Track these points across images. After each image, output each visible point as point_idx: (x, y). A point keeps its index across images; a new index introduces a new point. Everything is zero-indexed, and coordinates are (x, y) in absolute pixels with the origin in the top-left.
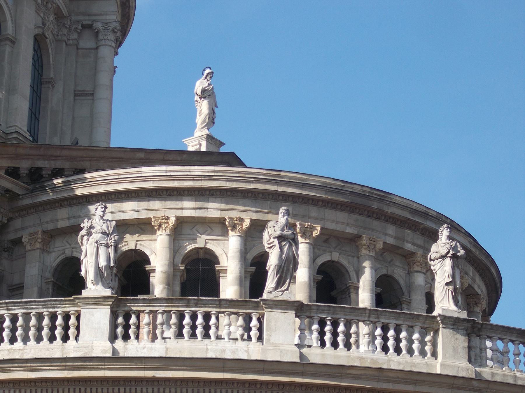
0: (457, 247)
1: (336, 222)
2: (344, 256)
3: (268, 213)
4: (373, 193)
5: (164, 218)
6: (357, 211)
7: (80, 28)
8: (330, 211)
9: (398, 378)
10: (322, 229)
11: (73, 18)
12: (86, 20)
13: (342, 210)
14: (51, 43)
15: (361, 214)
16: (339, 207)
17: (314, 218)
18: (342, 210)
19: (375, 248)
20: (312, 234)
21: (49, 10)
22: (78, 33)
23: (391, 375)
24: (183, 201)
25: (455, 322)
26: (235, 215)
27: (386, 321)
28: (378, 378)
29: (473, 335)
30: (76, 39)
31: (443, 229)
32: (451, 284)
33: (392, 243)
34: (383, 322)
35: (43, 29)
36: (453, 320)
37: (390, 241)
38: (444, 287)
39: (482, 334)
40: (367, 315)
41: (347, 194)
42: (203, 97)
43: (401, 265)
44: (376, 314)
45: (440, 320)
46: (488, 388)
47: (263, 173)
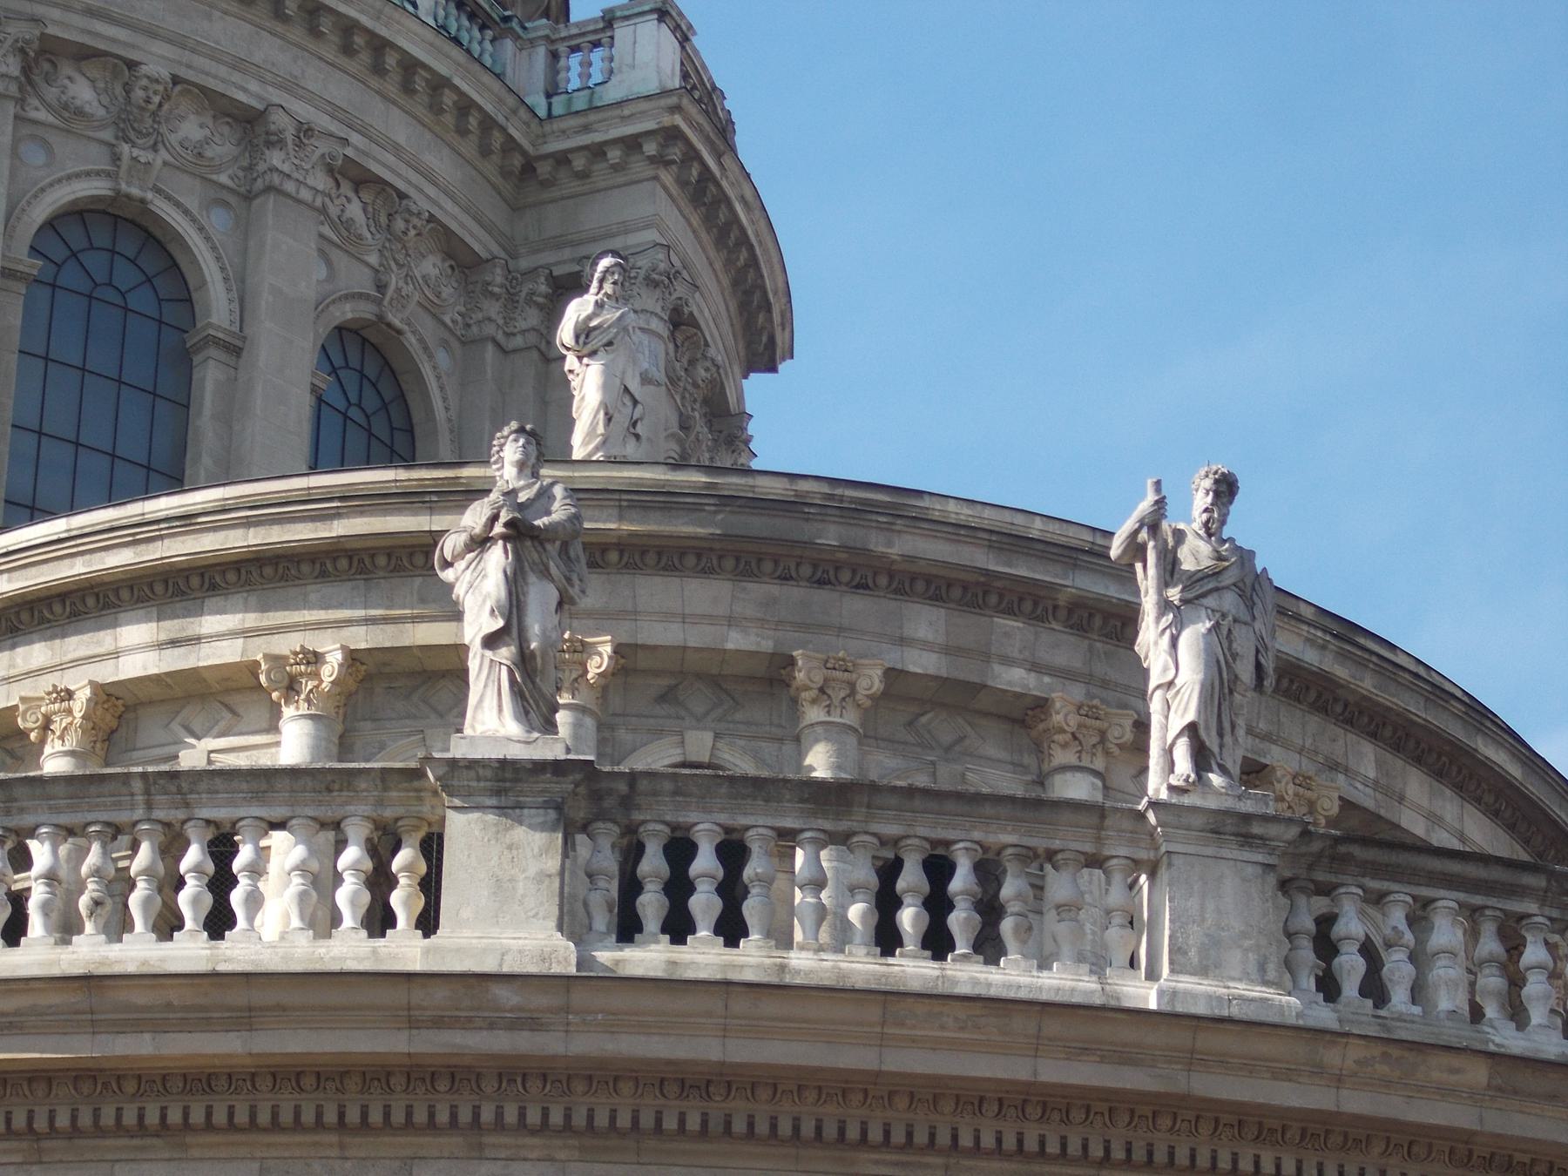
0: (552, 498)
1: (684, 619)
2: (742, 743)
3: (415, 619)
4: (841, 499)
5: (54, 695)
6: (768, 566)
7: (543, 288)
8: (657, 580)
9: (169, 1006)
10: (618, 650)
11: (524, 263)
12: (564, 262)
13: (707, 572)
14: (426, 349)
15: (786, 579)
16: (691, 560)
17: (590, 614)
18: (703, 571)
19: (853, 692)
20: (586, 672)
21: (399, 240)
22: (541, 307)
23: (140, 998)
24: (120, 626)
25: (504, 780)
26: (286, 645)
27: (222, 814)
28: (89, 1017)
29: (600, 824)
30: (533, 329)
31: (502, 440)
32: (507, 639)
33: (931, 671)
34: (208, 822)
35: (379, 302)
36: (489, 773)
37: (922, 662)
38: (483, 656)
39: (642, 818)
40: (140, 798)
41: (707, 508)
42: (586, 351)
43: (1003, 755)
44: (173, 789)
45: (437, 779)
46: (567, 1009)
47: (396, 481)
